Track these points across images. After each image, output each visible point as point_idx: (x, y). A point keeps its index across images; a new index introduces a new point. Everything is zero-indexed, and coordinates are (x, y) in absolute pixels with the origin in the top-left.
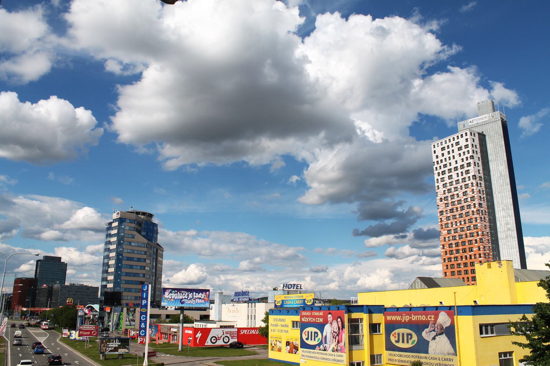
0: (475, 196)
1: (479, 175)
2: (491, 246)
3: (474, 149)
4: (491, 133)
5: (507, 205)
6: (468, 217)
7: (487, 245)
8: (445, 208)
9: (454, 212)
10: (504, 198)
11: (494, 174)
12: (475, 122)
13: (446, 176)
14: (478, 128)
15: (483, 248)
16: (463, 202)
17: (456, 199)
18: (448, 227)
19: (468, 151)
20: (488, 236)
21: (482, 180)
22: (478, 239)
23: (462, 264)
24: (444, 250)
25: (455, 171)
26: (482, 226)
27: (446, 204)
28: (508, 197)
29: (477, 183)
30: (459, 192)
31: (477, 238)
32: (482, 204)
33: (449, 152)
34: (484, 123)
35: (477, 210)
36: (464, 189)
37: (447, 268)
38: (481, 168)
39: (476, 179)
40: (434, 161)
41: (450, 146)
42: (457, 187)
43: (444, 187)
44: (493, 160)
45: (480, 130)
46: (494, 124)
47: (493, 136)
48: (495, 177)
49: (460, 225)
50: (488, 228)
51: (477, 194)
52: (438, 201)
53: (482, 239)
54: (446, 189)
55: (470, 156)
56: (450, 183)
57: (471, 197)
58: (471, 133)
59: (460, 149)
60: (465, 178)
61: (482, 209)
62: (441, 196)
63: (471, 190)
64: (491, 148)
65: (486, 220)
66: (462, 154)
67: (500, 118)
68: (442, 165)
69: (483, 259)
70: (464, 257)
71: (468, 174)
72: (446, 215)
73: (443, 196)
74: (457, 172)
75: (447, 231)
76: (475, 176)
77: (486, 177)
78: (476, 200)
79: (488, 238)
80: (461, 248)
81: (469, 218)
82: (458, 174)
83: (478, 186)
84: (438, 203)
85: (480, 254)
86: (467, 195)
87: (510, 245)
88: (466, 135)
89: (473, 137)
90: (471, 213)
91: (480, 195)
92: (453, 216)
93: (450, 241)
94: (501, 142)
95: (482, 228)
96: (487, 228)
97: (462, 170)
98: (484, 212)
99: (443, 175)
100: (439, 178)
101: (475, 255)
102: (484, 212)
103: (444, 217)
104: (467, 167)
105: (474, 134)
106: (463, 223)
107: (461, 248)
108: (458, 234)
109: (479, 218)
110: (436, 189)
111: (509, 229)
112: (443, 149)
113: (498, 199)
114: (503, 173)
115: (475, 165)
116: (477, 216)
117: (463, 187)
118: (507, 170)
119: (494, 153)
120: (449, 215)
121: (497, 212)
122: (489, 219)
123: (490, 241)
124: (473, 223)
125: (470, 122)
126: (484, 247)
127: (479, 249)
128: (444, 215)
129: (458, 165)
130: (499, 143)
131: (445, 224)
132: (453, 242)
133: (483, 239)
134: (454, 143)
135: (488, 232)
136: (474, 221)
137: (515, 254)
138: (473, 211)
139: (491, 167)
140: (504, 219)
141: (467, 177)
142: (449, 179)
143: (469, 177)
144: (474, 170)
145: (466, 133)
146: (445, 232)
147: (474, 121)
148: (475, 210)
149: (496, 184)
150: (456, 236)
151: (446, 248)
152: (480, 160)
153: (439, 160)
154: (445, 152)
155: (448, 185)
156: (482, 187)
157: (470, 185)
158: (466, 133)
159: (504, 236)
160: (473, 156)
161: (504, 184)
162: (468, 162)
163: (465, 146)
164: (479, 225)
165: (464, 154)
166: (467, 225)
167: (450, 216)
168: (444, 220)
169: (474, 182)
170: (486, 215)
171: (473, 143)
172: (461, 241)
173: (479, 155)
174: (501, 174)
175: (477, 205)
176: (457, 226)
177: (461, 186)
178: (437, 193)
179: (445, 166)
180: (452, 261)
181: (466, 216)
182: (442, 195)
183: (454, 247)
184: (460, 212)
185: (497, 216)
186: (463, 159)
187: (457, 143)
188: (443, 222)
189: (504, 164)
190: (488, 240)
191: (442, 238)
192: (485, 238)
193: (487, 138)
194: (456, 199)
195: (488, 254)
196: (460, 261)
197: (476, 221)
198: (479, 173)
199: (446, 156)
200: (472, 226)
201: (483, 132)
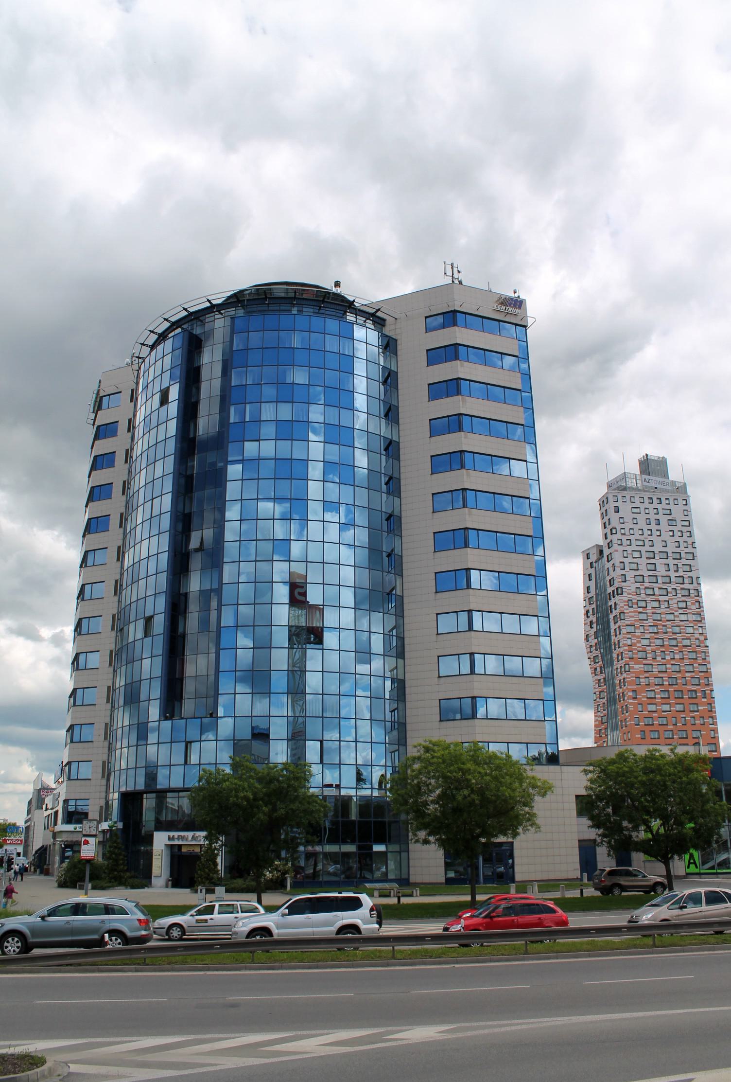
18: (646, 658)
54: (641, 585)
62: (631, 596)
73: (635, 598)
103: (638, 637)
132: (658, 689)
147: (650, 481)
151: (641, 698)
182: (633, 595)
183: (658, 698)
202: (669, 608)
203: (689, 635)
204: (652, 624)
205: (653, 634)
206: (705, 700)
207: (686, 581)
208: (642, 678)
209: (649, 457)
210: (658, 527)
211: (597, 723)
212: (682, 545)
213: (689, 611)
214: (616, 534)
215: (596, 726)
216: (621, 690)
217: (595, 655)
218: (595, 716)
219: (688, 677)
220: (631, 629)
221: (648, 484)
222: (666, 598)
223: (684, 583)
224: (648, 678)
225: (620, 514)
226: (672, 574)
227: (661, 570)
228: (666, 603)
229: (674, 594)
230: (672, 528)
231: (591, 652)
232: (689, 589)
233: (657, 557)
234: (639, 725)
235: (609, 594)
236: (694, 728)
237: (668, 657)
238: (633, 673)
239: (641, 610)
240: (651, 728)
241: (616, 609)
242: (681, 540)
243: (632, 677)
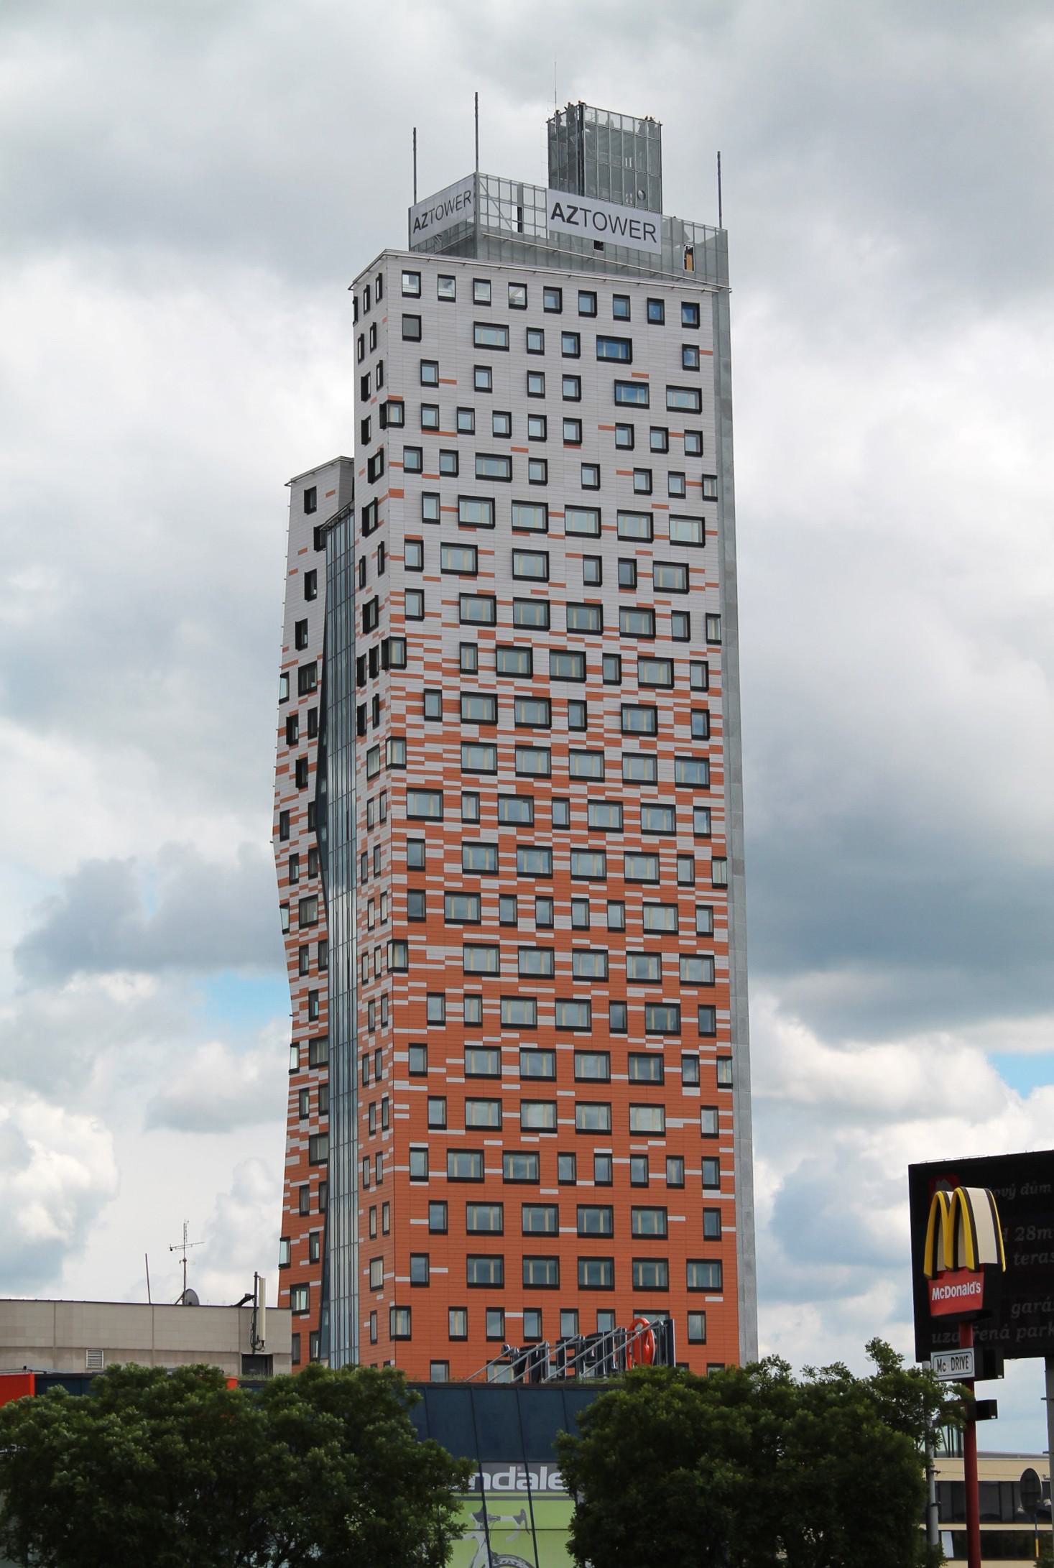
0: (713, 758)
30: (592, 696)
31: (702, 1048)
54: (482, 635)
62: (436, 675)
72: (465, 832)
73: (453, 686)
103: (451, 838)
108: (552, 991)
147: (578, 217)
151: (443, 1076)
172: (571, 1047)
176: (549, 935)
182: (447, 673)
183: (511, 1079)
196: (555, 1192)
202: (583, 729)
203: (655, 840)
204: (511, 790)
205: (511, 831)
207: (663, 627)
208: (455, 998)
209: (588, 116)
210: (573, 410)
211: (296, 1160)
212: (662, 483)
213: (663, 746)
214: (401, 425)
215: (290, 1172)
216: (372, 1042)
217: (305, 894)
218: (291, 1134)
219: (636, 1001)
220: (427, 806)
221: (567, 229)
222: (578, 691)
223: (652, 637)
224: (478, 996)
225: (426, 348)
226: (611, 597)
228: (576, 711)
229: (611, 676)
230: (626, 415)
231: (293, 881)
232: (671, 661)
233: (556, 526)
234: (425, 1179)
235: (361, 660)
236: (640, 1197)
237: (562, 923)
238: (419, 975)
239: (471, 731)
240: (475, 1192)
241: (376, 724)
242: (660, 466)
243: (413, 991)
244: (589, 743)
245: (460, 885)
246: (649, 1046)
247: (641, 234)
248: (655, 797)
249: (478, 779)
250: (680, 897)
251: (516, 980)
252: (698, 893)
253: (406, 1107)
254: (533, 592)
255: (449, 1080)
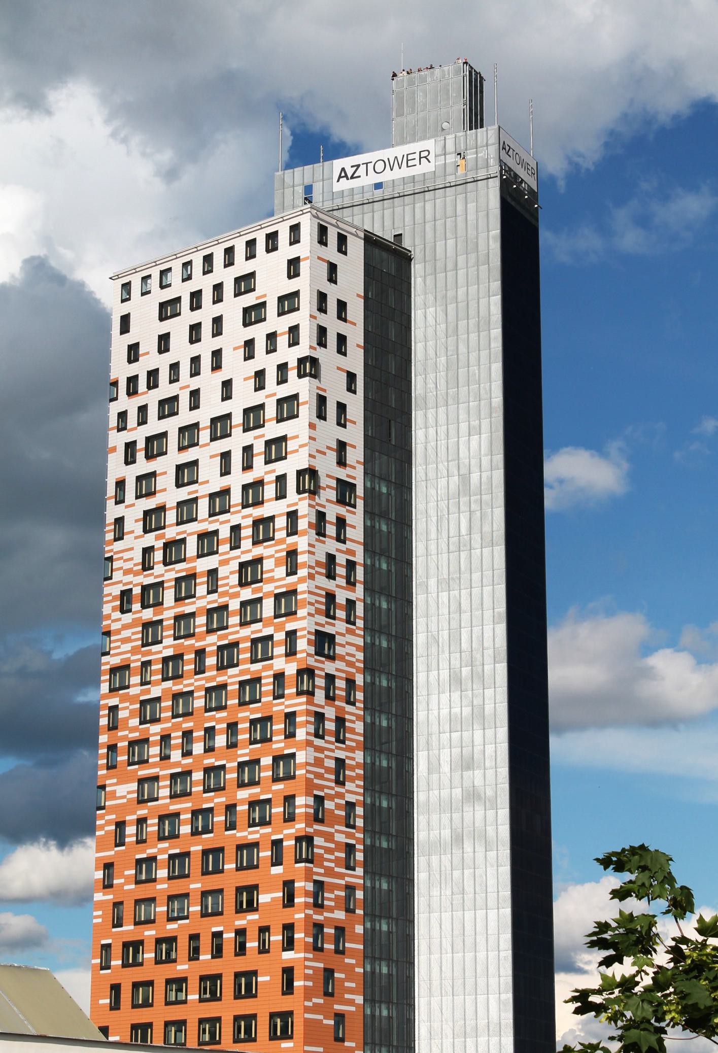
1: (342, 474)
2: (365, 888)
3: (330, 320)
4: (440, 245)
5: (478, 656)
6: (253, 711)
7: (341, 876)
8: (139, 653)
9: (181, 676)
10: (465, 617)
11: (431, 475)
12: (367, 180)
13: (166, 465)
14: (377, 215)
15: (307, 894)
16: (234, 620)
17: (203, 600)
18: (147, 761)
19: (294, 330)
20: (348, 826)
21: (354, 506)
22: (288, 837)
23: (194, 983)
24: (111, 897)
25: (214, 438)
26: (319, 762)
27: (146, 625)
28: (488, 614)
29: (321, 516)
31: (286, 832)
32: (338, 639)
33: (195, 332)
34: (409, 189)
35: (300, 672)
36: (246, 544)
37: (115, 1005)
38: (355, 435)
39: (314, 492)
40: (113, 376)
41: (207, 297)
42: (216, 532)
43: (151, 531)
44: (431, 402)
45: (388, 223)
46: (460, 198)
47: (450, 266)
48: (432, 491)
49: (206, 751)
50: (358, 777)
51: (311, 576)
52: (107, 609)
53: (309, 839)
54: (157, 538)
55: (301, 361)
56: (180, 504)
57: (278, 597)
58: (323, 231)
59: (254, 315)
60: (260, 483)
61: (330, 667)
62: (130, 578)
63: (284, 553)
64: (430, 331)
65: (353, 731)
66: (260, 346)
67: (495, 169)
68: (152, 399)
69: (302, 955)
70: (206, 942)
71: (277, 460)
72: (143, 692)
74: (222, 446)
75: (134, 786)
76: (312, 473)
77: (384, 490)
78: (301, 613)
79: (348, 835)
80: (199, 885)
81: (252, 717)
82: (226, 456)
83: (324, 535)
84: (108, 617)
85: (289, 928)
86: (261, 581)
87: (469, 888)
88: (295, 239)
89: (331, 252)
90: (267, 685)
91: (330, 585)
92: (176, 696)
93: (144, 841)
94: (483, 302)
95: (319, 776)
96: (352, 779)
97: (248, 438)
98: (340, 684)
99: (149, 456)
100: (131, 473)
101: (264, 930)
102: (340, 684)
104: (280, 419)
105: (342, 240)
106: (220, 741)
107: (199, 885)
108: (189, 805)
109: (303, 718)
110: (110, 536)
111: (472, 796)
112: (168, 309)
113: (434, 619)
114: (475, 477)
115: (321, 415)
116: (298, 704)
117: (247, 532)
118: (499, 458)
119: (443, 359)
120: (155, 692)
121: (425, 692)
122: (370, 731)
123: (360, 856)
124: (274, 746)
125: (343, 174)
126: (319, 885)
127: (289, 900)
128: (133, 691)
129: (236, 408)
130: (473, 305)
131: (132, 743)
133: (318, 841)
134: (226, 276)
135: (350, 806)
136: (278, 732)
137: (492, 939)
138: (279, 677)
139: (419, 435)
140: (456, 735)
141: (272, 477)
142: (179, 484)
143: (281, 480)
144: (310, 438)
145: (295, 229)
146: (125, 790)
147: (361, 171)
148: (291, 669)
149: (433, 535)
150: (177, 815)
151: (122, 885)
152: (354, 392)
153: (140, 369)
154: (178, 328)
155: (171, 517)
156: (349, 545)
157: (281, 522)
158: (295, 229)
159: (446, 833)
160: (314, 361)
161: (476, 537)
162: (284, 391)
163: (281, 299)
164: (301, 757)
165: (271, 349)
166: (244, 753)
167: (158, 699)
168: (126, 720)
169: (304, 507)
170: (353, 704)
171: (327, 288)
172: (200, 848)
173: (355, 361)
174: (465, 480)
175: (302, 644)
176: (189, 760)
177: (236, 529)
178: (110, 559)
179: (168, 407)
180: (141, 964)
181: (242, 704)
182: (136, 574)
184: (212, 679)
185: (420, 715)
186: (260, 375)
187: (245, 283)
188: (120, 734)
189: (485, 423)
190: (350, 849)
191: (105, 824)
192: (332, 835)
193: (417, 269)
194: (203, 600)
195: (336, 928)
196: (186, 967)
197: (290, 735)
198: (342, 462)
199: (181, 350)
200: (267, 761)
201: (398, 237)
206: (277, 870)
227: (209, 472)
244: (220, 600)
245: (137, 734)
246: (250, 837)
247: (417, 162)
248: (260, 631)
249: (151, 650)
250: (275, 709)
251: (168, 801)
252: (287, 703)
253: (100, 913)
254: (189, 493)
255: (126, 887)
